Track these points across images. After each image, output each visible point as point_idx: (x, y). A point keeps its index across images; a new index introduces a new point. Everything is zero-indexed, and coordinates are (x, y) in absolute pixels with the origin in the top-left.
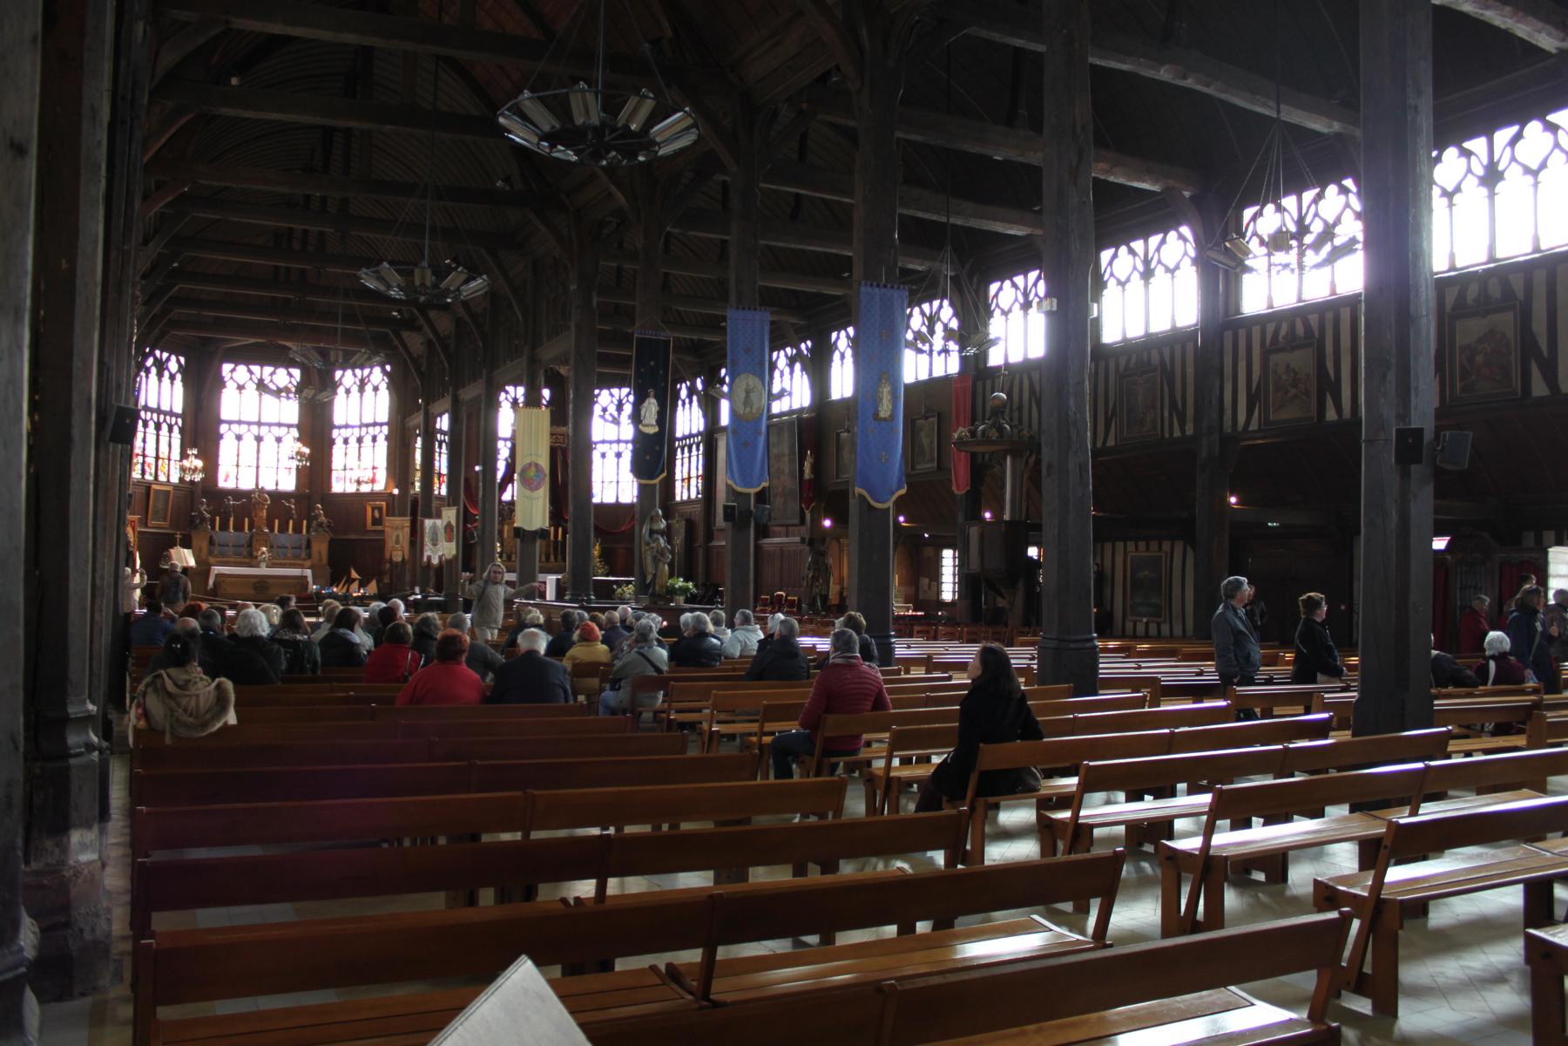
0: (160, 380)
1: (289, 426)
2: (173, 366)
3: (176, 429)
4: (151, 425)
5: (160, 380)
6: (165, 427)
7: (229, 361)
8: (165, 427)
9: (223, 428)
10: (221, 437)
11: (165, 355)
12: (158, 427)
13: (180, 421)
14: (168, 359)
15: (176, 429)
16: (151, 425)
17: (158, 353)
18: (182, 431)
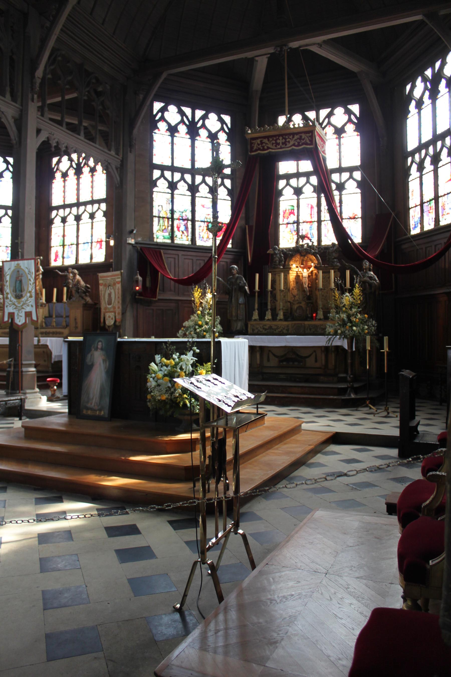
0: (193, 140)
1: (351, 170)
2: (213, 122)
3: (222, 193)
4: (182, 188)
5: (193, 140)
6: (204, 190)
7: (282, 113)
8: (204, 190)
9: (282, 183)
10: (280, 193)
11: (199, 113)
12: (193, 189)
13: (228, 183)
14: (204, 118)
15: (222, 193)
16: (182, 188)
17: (188, 111)
18: (230, 193)
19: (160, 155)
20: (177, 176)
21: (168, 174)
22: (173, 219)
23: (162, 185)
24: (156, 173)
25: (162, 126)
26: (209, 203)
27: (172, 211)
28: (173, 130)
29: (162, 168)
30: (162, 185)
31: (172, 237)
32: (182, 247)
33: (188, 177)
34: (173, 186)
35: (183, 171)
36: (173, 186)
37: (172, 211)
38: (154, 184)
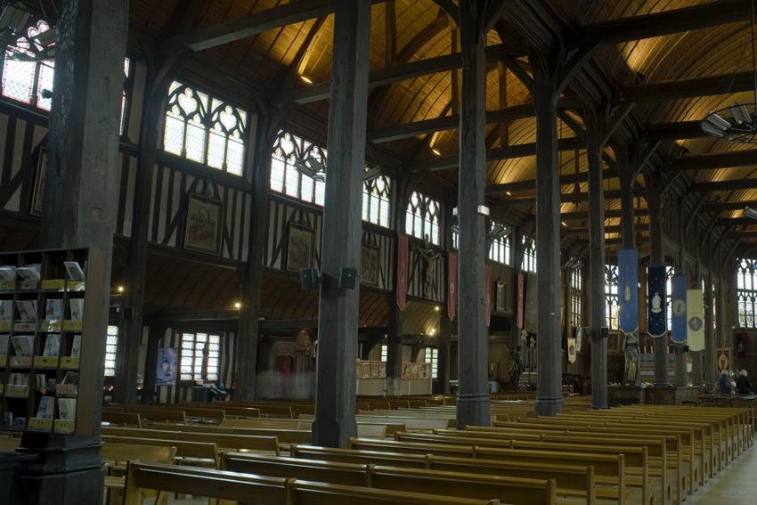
4: (749, 299)
16: (749, 299)
17: (749, 261)
19: (740, 286)
20: (747, 294)
21: (743, 293)
22: (746, 315)
23: (741, 298)
24: (739, 293)
25: (740, 269)
26: (751, 305)
27: (746, 312)
28: (744, 271)
29: (741, 291)
30: (741, 298)
31: (746, 324)
32: (750, 329)
33: (751, 294)
34: (745, 299)
35: (748, 291)
36: (745, 299)
37: (746, 312)
38: (738, 298)
